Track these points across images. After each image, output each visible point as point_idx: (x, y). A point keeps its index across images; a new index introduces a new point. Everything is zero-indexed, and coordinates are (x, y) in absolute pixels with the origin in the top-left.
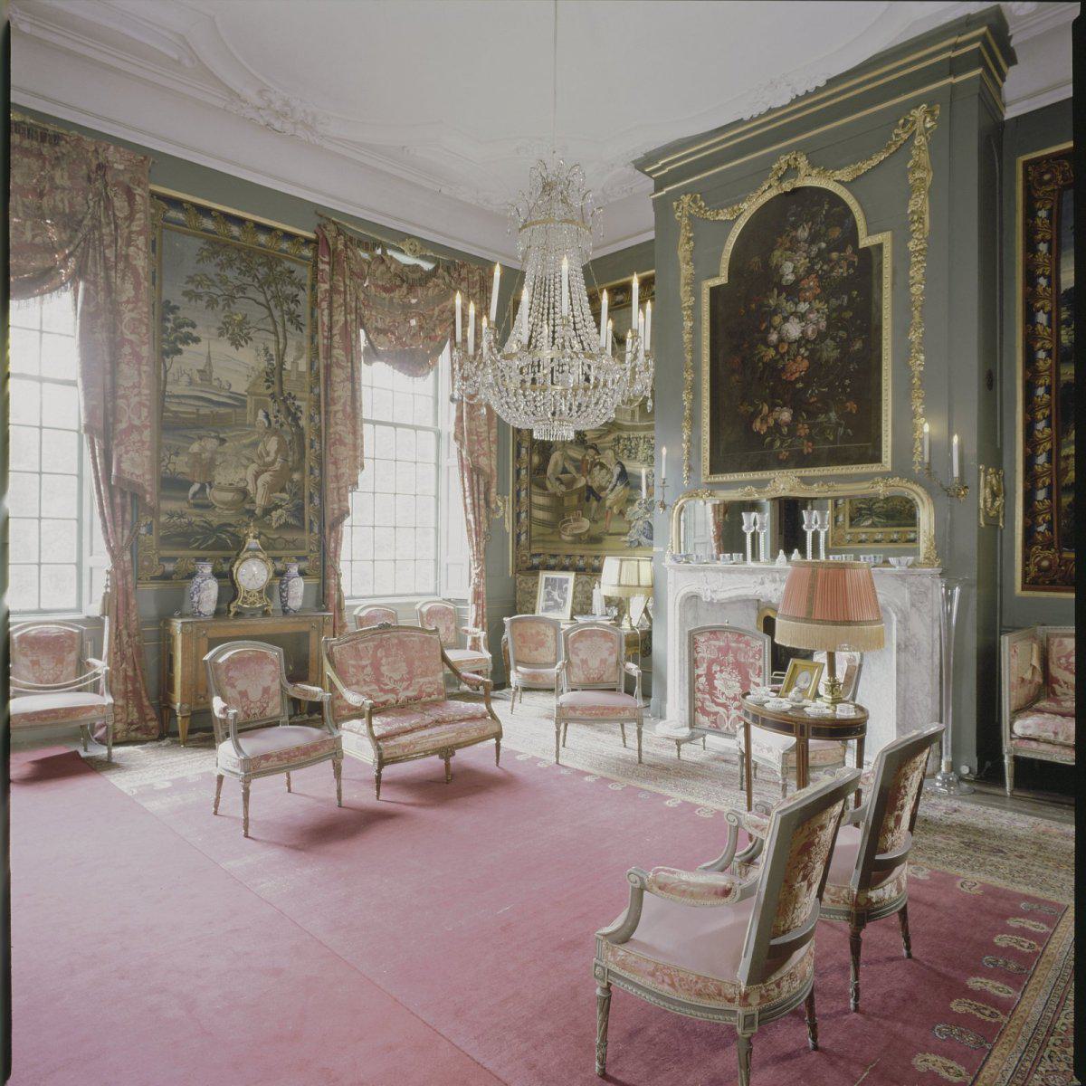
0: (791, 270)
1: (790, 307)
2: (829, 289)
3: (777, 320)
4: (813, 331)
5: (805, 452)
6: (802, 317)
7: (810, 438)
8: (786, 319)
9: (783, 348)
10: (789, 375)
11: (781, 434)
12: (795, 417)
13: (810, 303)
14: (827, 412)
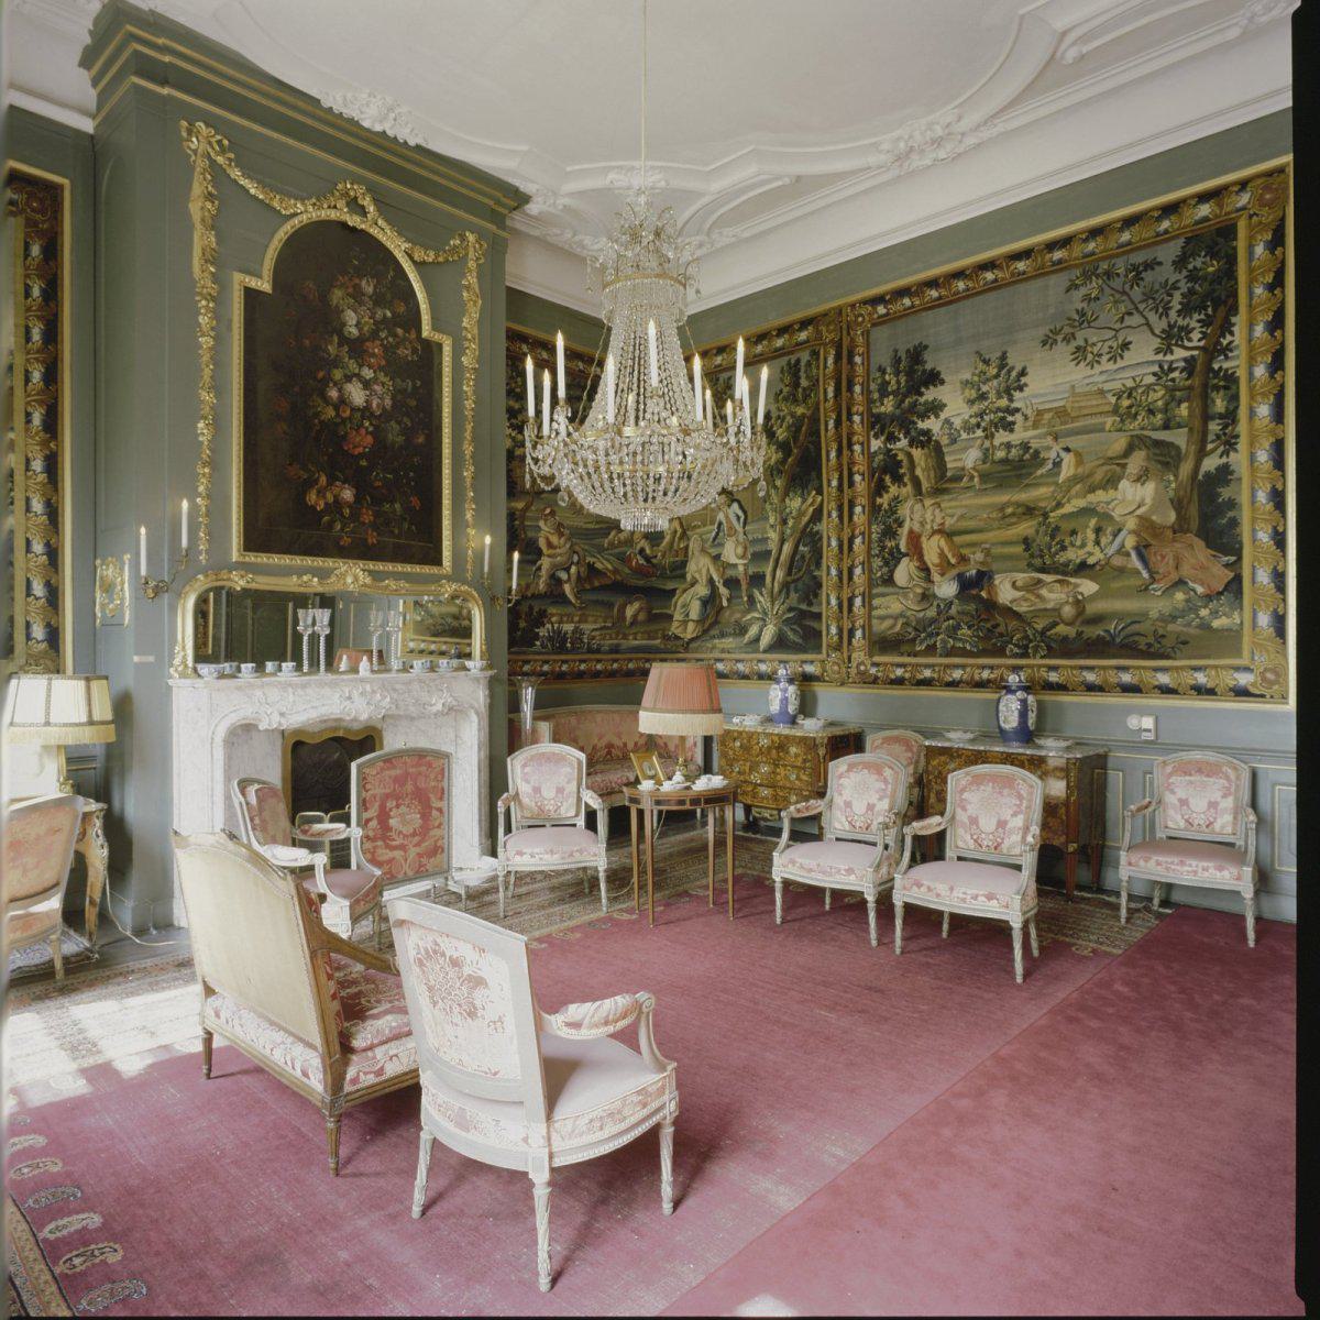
0: (354, 322)
1: (353, 366)
2: (393, 367)
3: (338, 374)
4: (378, 405)
5: (370, 541)
6: (366, 384)
7: (374, 526)
8: (348, 379)
9: (345, 412)
10: (351, 446)
11: (342, 515)
12: (358, 498)
13: (375, 372)
14: (392, 502)
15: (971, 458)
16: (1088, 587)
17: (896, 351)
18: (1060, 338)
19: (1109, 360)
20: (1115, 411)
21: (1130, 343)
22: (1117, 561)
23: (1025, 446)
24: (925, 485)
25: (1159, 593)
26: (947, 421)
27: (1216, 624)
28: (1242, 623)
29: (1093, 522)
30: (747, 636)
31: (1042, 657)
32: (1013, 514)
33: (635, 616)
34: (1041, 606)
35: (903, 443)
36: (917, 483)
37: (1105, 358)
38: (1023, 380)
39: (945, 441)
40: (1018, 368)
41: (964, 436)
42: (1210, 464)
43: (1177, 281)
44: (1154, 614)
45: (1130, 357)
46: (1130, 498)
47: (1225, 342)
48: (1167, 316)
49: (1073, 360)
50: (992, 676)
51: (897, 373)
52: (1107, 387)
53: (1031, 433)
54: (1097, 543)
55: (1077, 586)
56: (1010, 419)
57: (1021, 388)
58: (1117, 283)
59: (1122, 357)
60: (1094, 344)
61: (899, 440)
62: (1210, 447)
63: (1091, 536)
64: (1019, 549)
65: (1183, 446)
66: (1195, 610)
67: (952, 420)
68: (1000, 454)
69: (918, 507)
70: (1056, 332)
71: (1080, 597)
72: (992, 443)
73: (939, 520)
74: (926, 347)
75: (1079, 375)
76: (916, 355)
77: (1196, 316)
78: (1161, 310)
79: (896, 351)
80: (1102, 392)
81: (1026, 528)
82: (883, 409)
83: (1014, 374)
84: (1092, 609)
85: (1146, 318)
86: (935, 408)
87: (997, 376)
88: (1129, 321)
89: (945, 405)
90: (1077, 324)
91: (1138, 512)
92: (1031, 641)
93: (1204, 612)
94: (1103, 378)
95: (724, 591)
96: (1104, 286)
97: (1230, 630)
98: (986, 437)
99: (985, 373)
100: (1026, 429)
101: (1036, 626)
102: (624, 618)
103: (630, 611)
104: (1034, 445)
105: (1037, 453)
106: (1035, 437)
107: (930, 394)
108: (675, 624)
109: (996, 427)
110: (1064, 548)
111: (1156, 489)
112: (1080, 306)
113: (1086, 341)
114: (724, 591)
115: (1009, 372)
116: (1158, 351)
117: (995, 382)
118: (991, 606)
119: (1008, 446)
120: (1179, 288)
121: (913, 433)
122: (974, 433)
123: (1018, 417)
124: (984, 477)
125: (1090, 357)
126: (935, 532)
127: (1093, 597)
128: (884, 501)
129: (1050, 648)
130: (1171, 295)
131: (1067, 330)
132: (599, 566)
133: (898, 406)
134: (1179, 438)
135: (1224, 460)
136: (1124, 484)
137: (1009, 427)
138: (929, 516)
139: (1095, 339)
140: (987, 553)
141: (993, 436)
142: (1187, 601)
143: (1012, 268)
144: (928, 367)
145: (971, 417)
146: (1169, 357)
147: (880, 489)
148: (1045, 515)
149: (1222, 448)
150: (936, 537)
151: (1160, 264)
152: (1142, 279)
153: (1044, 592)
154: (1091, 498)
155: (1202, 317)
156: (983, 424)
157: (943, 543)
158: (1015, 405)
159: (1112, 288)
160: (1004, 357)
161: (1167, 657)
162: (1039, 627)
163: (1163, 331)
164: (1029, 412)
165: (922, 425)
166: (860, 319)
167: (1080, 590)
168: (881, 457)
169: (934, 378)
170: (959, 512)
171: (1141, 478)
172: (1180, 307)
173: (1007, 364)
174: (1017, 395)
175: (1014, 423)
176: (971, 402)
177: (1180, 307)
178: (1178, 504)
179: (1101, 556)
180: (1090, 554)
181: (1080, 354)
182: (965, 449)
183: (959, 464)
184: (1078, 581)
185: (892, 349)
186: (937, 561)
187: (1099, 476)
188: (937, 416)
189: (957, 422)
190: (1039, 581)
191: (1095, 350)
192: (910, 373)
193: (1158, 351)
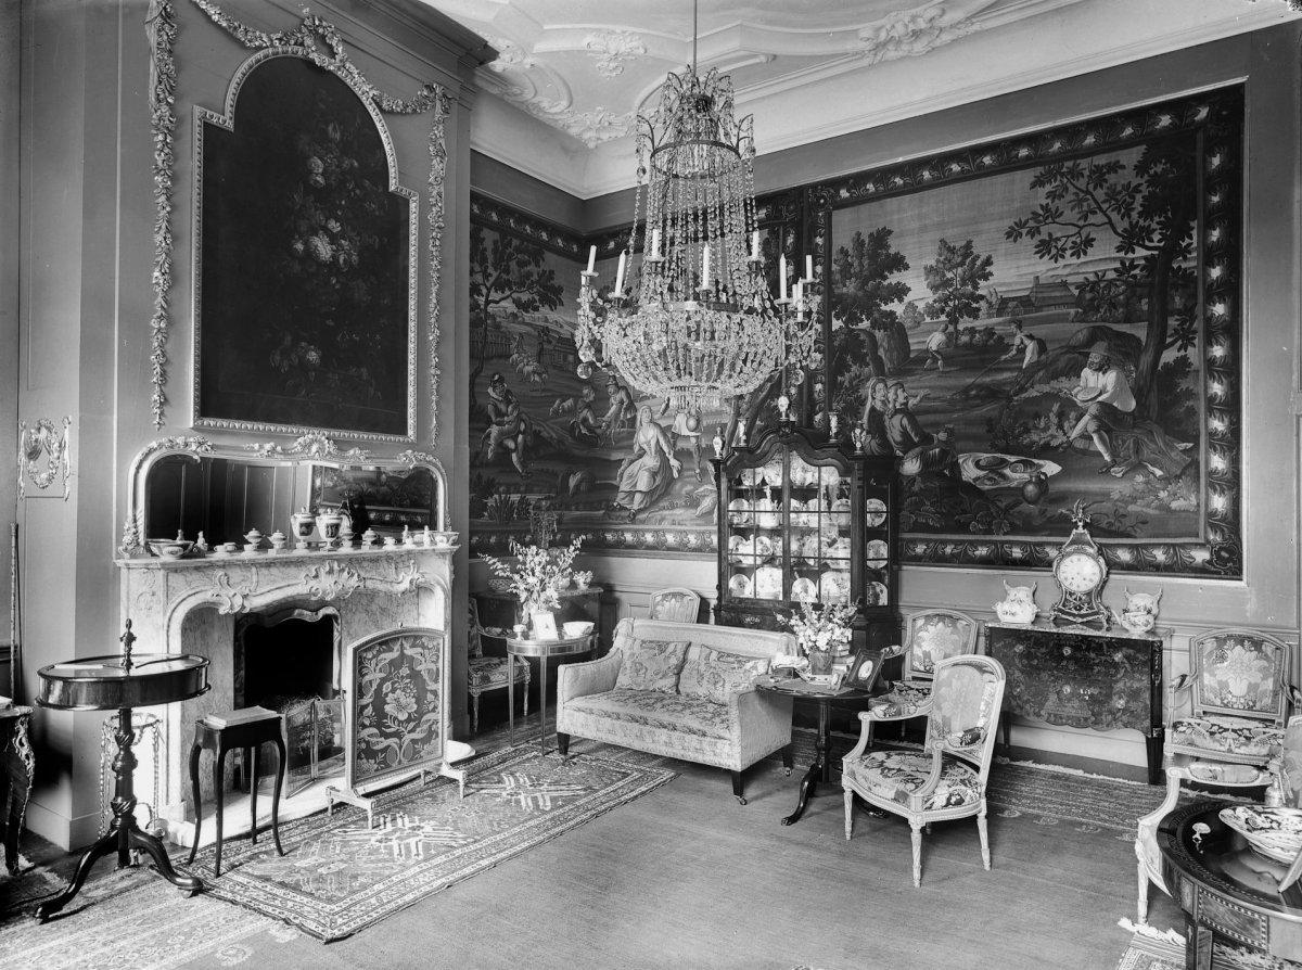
15: (935, 340)
16: (1051, 468)
17: (859, 234)
18: (1024, 231)
19: (1072, 255)
20: (1078, 302)
21: (1093, 240)
22: (1080, 444)
23: (989, 332)
24: (888, 366)
25: (1120, 475)
26: (911, 305)
27: (1174, 505)
28: (1198, 505)
29: (1056, 408)
30: (699, 509)
31: (1005, 534)
32: (976, 396)
33: (577, 486)
34: (1004, 484)
35: (865, 324)
36: (879, 363)
37: (1069, 252)
38: (988, 269)
39: (908, 324)
40: (983, 257)
41: (928, 320)
42: (1169, 356)
43: (1140, 185)
44: (1115, 496)
45: (1094, 253)
46: (1091, 384)
47: (1184, 244)
48: (1129, 217)
49: (1037, 253)
50: (955, 551)
51: (861, 257)
52: (1070, 279)
53: (995, 320)
54: (1060, 426)
55: (1041, 466)
56: (974, 305)
57: (986, 277)
58: (1082, 183)
59: (1085, 253)
60: (1058, 239)
61: (862, 321)
62: (1169, 340)
63: (1054, 420)
64: (982, 430)
65: (1143, 339)
66: (1155, 492)
67: (916, 303)
68: (965, 339)
69: (881, 385)
70: (1021, 225)
71: (1043, 477)
72: (956, 328)
73: (901, 399)
74: (890, 232)
75: (1044, 268)
76: (881, 238)
77: (1157, 219)
78: (1123, 210)
79: (859, 234)
80: (1064, 285)
81: (989, 410)
82: (845, 290)
83: (978, 263)
84: (1055, 488)
85: (1108, 217)
86: (900, 292)
87: (962, 264)
88: (1092, 219)
89: (909, 289)
90: (1041, 218)
91: (1100, 399)
92: (995, 518)
93: (1163, 494)
94: (1068, 271)
95: (674, 463)
96: (1069, 185)
97: (1188, 511)
98: (950, 322)
99: (950, 261)
100: (990, 316)
101: (999, 504)
102: (568, 487)
103: (573, 482)
104: (999, 330)
105: (1001, 338)
106: (999, 324)
107: (894, 278)
108: (621, 495)
109: (960, 312)
110: (1027, 431)
111: (1118, 378)
112: (1044, 202)
113: (1050, 235)
114: (674, 463)
115: (974, 261)
116: (1119, 249)
117: (960, 269)
118: (956, 483)
119: (972, 331)
120: (1141, 191)
121: (876, 315)
122: (938, 318)
123: (983, 304)
124: (948, 360)
125: (1054, 251)
126: (897, 412)
127: (1055, 478)
128: (845, 379)
129: (1012, 524)
130: (1134, 198)
131: (1032, 224)
132: (544, 434)
133: (862, 287)
134: (1140, 331)
135: (1182, 353)
136: (1086, 372)
137: (974, 313)
138: (891, 396)
139: (1059, 235)
140: (950, 432)
141: (957, 323)
142: (1147, 483)
143: (978, 161)
144: (892, 251)
145: (935, 301)
146: (1130, 255)
147: (842, 368)
148: (1010, 399)
149: (1180, 342)
150: (899, 416)
151: (1123, 167)
152: (1106, 181)
153: (1007, 471)
154: (1054, 383)
155: (1162, 219)
156: (947, 309)
157: (905, 421)
158: (980, 292)
159: (1077, 188)
160: (969, 245)
161: (1129, 536)
162: (1002, 505)
163: (1125, 230)
164: (994, 300)
165: (884, 307)
166: (822, 201)
167: (1043, 470)
168: (843, 337)
169: (899, 263)
170: (922, 393)
171: (1102, 368)
172: (1140, 209)
173: (972, 253)
174: (982, 283)
175: (978, 309)
176: (935, 288)
177: (1140, 209)
178: (1138, 393)
179: (1065, 439)
180: (1053, 437)
181: (1044, 248)
182: (929, 332)
183: (924, 347)
184: (1041, 462)
185: (854, 232)
186: (899, 439)
187: (1061, 364)
188: (901, 300)
189: (921, 306)
190: (1003, 462)
191: (1060, 244)
192: (874, 256)
193: (1119, 249)
